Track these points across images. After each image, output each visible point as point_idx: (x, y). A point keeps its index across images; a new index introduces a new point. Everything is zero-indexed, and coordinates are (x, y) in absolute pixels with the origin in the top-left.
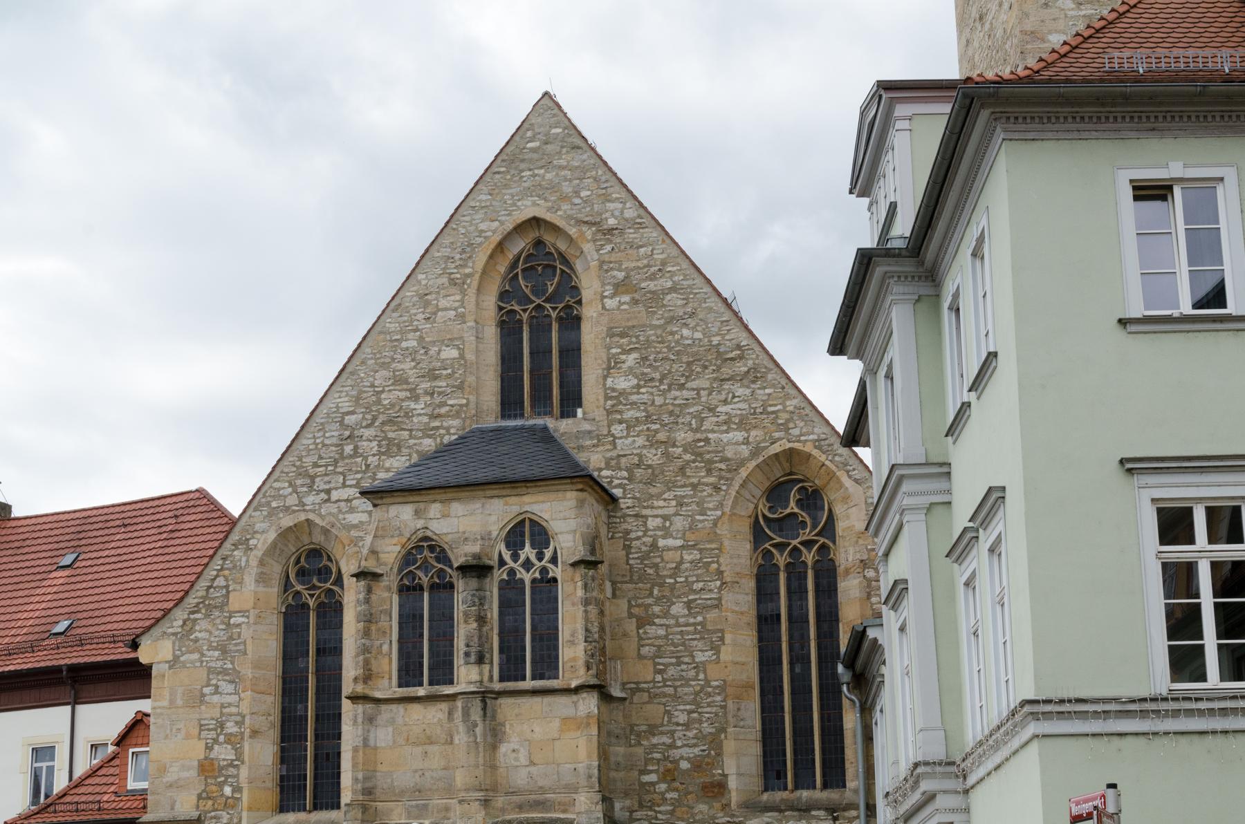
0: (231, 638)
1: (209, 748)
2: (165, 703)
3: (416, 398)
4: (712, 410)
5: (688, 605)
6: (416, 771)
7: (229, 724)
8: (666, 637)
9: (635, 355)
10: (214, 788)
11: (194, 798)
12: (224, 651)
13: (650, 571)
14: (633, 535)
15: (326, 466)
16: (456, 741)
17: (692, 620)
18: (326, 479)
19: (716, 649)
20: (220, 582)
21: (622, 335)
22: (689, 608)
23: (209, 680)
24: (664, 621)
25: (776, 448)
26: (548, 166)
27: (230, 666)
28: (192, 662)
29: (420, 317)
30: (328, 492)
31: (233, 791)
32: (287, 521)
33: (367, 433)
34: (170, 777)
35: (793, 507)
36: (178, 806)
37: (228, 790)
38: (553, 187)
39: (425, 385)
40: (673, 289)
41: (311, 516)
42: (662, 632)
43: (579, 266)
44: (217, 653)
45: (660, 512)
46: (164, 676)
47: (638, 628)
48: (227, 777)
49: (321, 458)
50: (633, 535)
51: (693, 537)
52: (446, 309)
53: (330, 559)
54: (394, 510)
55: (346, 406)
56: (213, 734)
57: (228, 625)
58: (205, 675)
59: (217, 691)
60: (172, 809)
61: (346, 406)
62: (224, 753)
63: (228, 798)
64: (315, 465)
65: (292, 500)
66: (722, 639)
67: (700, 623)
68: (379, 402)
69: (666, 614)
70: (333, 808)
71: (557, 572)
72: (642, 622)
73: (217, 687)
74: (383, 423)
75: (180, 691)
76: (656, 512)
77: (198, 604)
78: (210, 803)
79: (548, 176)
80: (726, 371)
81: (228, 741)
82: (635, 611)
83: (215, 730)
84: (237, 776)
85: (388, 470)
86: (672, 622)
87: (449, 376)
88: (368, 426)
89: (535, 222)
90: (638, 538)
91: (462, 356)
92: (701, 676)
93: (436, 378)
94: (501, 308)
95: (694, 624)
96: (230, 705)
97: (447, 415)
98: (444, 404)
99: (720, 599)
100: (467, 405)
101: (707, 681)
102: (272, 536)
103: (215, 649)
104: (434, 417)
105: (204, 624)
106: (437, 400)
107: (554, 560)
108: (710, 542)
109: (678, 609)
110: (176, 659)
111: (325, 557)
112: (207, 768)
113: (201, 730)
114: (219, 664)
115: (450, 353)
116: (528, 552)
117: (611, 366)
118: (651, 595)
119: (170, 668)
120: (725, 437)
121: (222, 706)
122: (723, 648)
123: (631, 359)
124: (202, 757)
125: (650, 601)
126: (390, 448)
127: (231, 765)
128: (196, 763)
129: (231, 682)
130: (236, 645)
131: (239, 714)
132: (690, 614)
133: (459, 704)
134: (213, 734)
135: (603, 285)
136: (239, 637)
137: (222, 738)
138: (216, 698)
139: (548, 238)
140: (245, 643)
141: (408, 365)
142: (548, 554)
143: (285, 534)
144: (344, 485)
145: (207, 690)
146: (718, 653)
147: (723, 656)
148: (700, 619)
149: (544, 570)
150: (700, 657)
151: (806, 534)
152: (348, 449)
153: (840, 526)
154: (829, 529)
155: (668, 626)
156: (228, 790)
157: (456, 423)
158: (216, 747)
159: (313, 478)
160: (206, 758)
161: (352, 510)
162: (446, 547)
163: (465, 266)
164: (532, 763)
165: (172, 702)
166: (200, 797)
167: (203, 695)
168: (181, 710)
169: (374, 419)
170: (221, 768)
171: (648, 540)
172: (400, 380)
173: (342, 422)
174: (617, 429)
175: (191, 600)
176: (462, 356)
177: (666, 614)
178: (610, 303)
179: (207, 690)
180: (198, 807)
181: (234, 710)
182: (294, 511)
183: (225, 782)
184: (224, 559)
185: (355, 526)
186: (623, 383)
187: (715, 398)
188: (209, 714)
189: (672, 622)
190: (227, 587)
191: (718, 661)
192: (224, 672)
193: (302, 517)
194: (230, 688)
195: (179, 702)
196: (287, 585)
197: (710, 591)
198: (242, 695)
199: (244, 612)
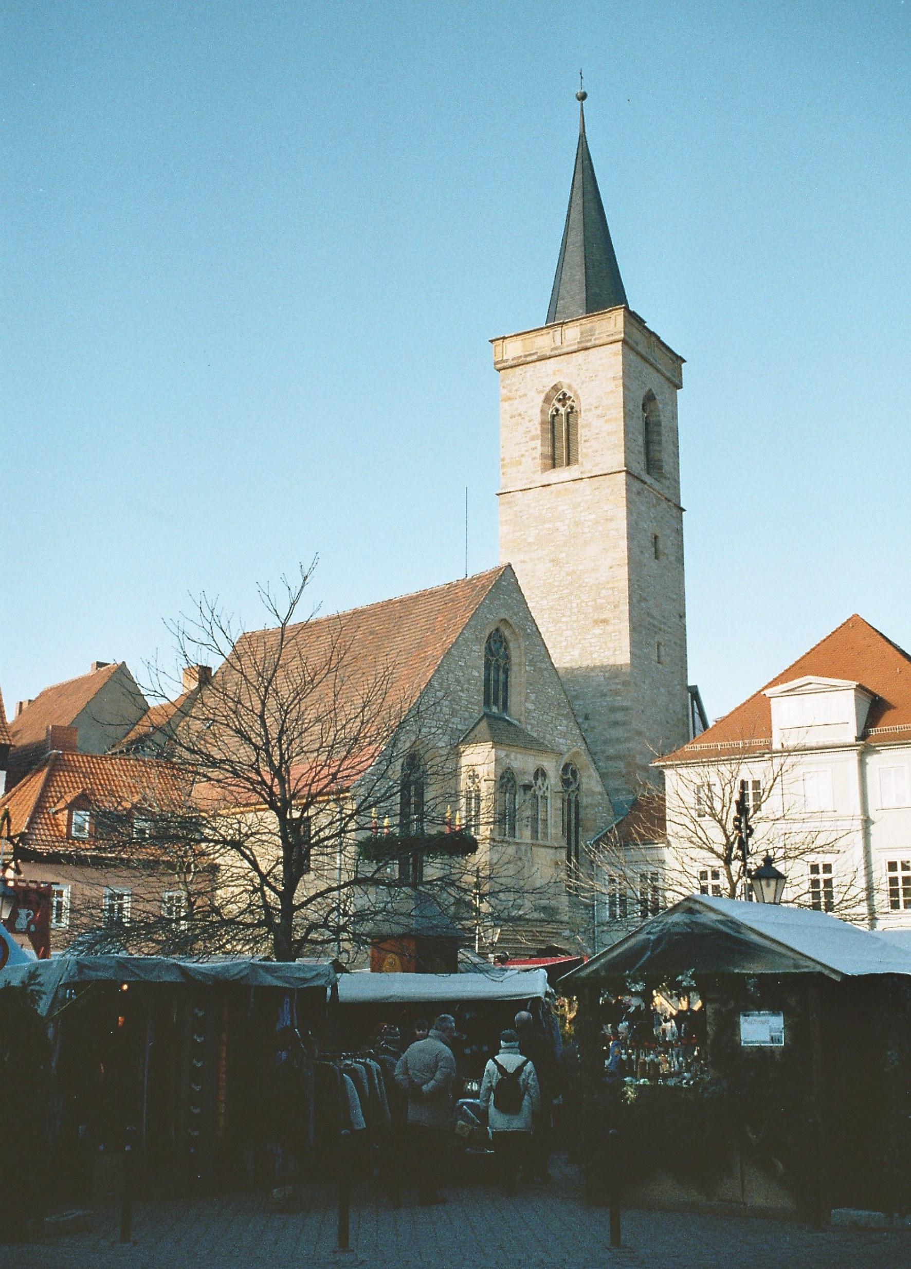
3: (462, 691)
4: (556, 727)
21: (531, 684)
26: (509, 596)
35: (570, 776)
40: (546, 669)
43: (511, 645)
54: (499, 752)
68: (449, 688)
71: (548, 794)
79: (510, 601)
89: (505, 620)
115: (476, 674)
116: (540, 782)
120: (561, 740)
123: (533, 697)
126: (454, 713)
139: (502, 628)
149: (544, 792)
151: (573, 787)
153: (584, 787)
154: (578, 789)
157: (476, 707)
174: (529, 727)
178: (528, 668)
186: (531, 706)
187: (557, 723)
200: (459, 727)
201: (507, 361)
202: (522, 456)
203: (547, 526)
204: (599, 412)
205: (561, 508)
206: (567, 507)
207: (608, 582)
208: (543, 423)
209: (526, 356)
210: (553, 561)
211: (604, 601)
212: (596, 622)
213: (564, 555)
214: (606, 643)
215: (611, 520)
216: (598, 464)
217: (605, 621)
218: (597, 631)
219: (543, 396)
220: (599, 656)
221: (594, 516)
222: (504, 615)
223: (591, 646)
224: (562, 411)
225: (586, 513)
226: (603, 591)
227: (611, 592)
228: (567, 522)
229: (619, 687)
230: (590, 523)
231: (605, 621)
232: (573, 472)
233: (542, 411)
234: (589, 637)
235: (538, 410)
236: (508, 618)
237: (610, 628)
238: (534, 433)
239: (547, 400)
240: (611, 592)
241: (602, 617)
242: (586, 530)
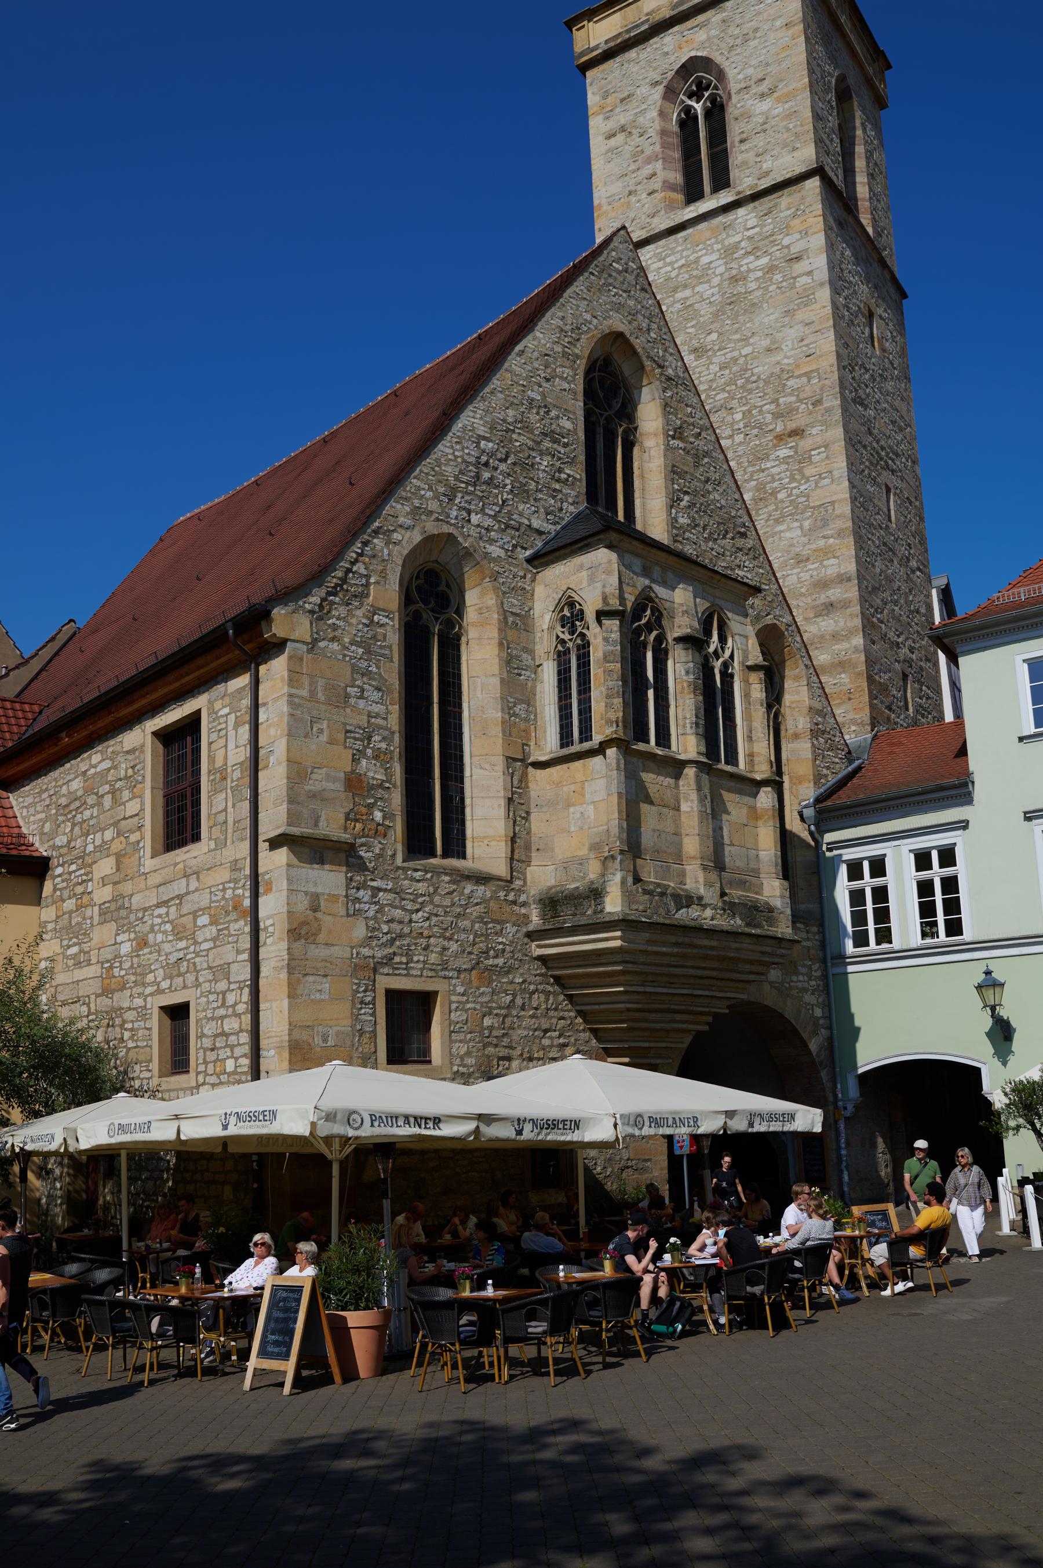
0: (374, 637)
1: (355, 760)
2: (304, 693)
6: (654, 831)
7: (377, 738)
9: (687, 498)
10: (364, 810)
11: (342, 816)
12: (368, 651)
16: (684, 807)
20: (360, 568)
23: (354, 680)
25: (769, 620)
27: (373, 669)
31: (384, 818)
34: (312, 786)
36: (322, 823)
37: (378, 816)
41: (455, 533)
44: (360, 651)
46: (301, 659)
48: (377, 799)
53: (448, 586)
56: (358, 745)
57: (372, 621)
58: (349, 673)
59: (361, 697)
60: (316, 825)
62: (371, 771)
63: (379, 824)
70: (458, 857)
75: (321, 683)
77: (337, 585)
78: (359, 826)
80: (740, 542)
81: (376, 757)
83: (362, 741)
84: (388, 801)
85: (521, 514)
102: (417, 538)
103: (358, 644)
107: (732, 657)
111: (444, 582)
112: (354, 783)
113: (346, 738)
114: (364, 664)
117: (673, 502)
119: (310, 651)
121: (369, 715)
124: (349, 769)
127: (381, 786)
128: (342, 775)
129: (378, 689)
130: (381, 647)
131: (386, 729)
133: (690, 772)
134: (358, 745)
136: (384, 640)
137: (369, 752)
138: (362, 703)
140: (390, 647)
142: (727, 654)
143: (430, 540)
145: (352, 691)
156: (378, 816)
158: (364, 762)
160: (353, 772)
162: (665, 612)
164: (732, 844)
165: (313, 692)
167: (347, 696)
168: (323, 707)
170: (372, 787)
175: (332, 581)
180: (346, 829)
181: (380, 721)
184: (366, 544)
193: (446, 529)
194: (376, 695)
195: (321, 696)
198: (390, 707)
200: (536, 524)
201: (596, 48)
202: (630, 193)
203: (679, 295)
204: (764, 87)
205: (705, 260)
206: (714, 257)
207: (798, 366)
208: (663, 133)
209: (628, 31)
210: (695, 350)
211: (793, 399)
212: (780, 438)
213: (714, 336)
214: (800, 471)
215: (798, 259)
216: (767, 173)
217: (797, 433)
218: (783, 452)
219: (661, 89)
220: (789, 496)
221: (765, 260)
223: (773, 480)
224: (698, 107)
225: (752, 258)
226: (789, 383)
227: (805, 379)
228: (716, 281)
229: (831, 541)
230: (760, 274)
231: (797, 433)
232: (725, 197)
233: (662, 114)
234: (769, 465)
235: (654, 113)
236: (627, 334)
237: (805, 444)
238: (648, 152)
239: (670, 93)
240: (805, 379)
241: (791, 426)
242: (753, 286)
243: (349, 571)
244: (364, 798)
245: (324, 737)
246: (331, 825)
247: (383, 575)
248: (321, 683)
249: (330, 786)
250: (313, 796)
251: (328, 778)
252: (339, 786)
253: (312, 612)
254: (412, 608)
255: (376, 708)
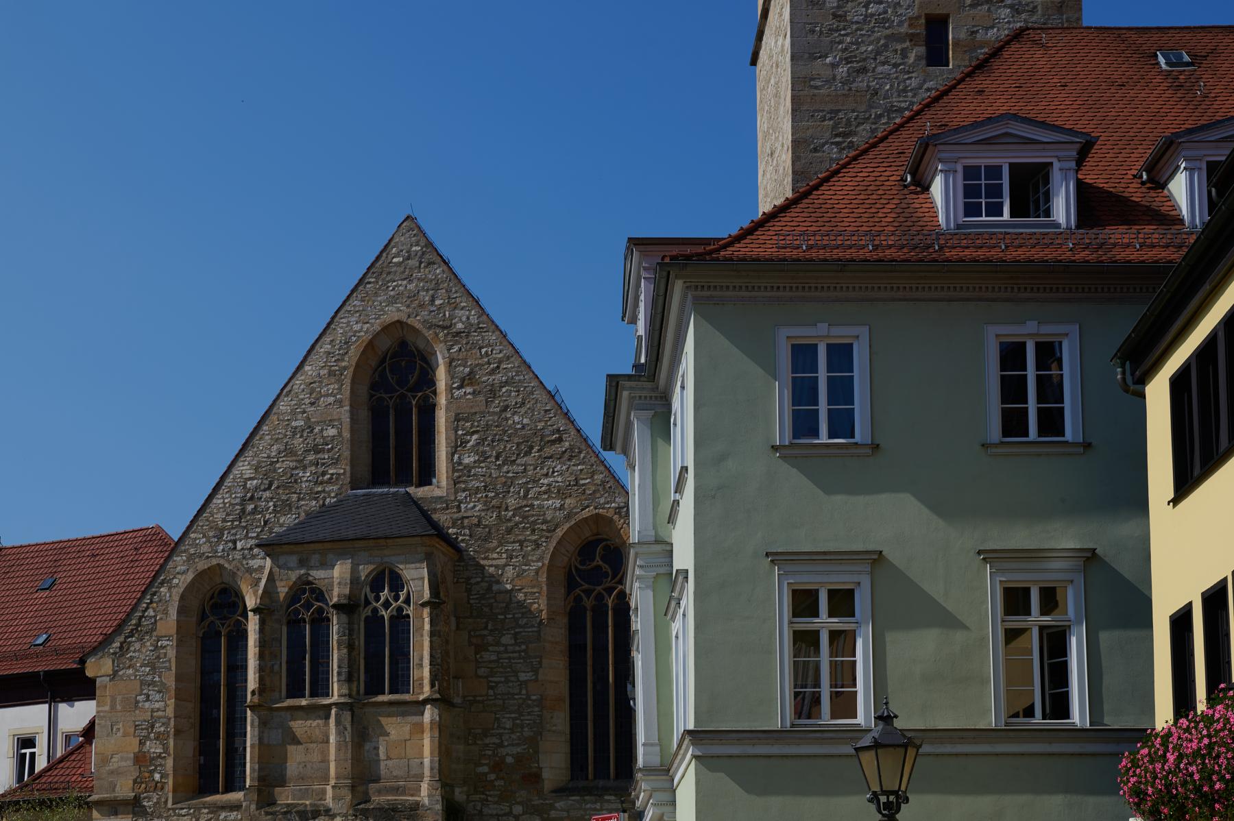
0: (158, 657)
1: (142, 743)
2: (107, 708)
5: (515, 636)
8: (497, 661)
10: (147, 775)
12: (154, 668)
13: (486, 609)
14: (473, 581)
15: (232, 521)
17: (517, 648)
18: (233, 531)
19: (536, 671)
20: (151, 612)
22: (516, 639)
24: (496, 648)
27: (157, 679)
28: (129, 676)
29: (307, 401)
30: (235, 542)
32: (202, 565)
33: (268, 494)
36: (118, 788)
37: (157, 776)
38: (413, 296)
39: (311, 457)
41: (222, 562)
42: (493, 657)
45: (495, 562)
47: (476, 653)
49: (228, 515)
50: (473, 581)
51: (519, 583)
52: (327, 395)
55: (248, 473)
59: (148, 699)
60: (114, 791)
61: (248, 473)
62: (153, 748)
64: (224, 521)
65: (205, 549)
66: (540, 663)
67: (524, 651)
68: (275, 470)
69: (498, 644)
72: (480, 648)
73: (148, 696)
74: (278, 487)
75: (119, 698)
76: (490, 562)
81: (157, 739)
82: (474, 640)
85: (281, 526)
86: (502, 649)
87: (329, 451)
88: (265, 490)
90: (478, 583)
91: (340, 434)
92: (524, 692)
93: (317, 452)
94: (372, 396)
95: (519, 652)
96: (158, 710)
97: (329, 481)
98: (324, 474)
99: (539, 632)
100: (344, 474)
101: (528, 698)
102: (190, 577)
103: (146, 665)
104: (316, 483)
105: (137, 645)
106: (321, 470)
108: (533, 587)
109: (507, 639)
110: (115, 673)
112: (141, 759)
115: (332, 432)
118: (486, 628)
121: (153, 711)
122: (541, 671)
125: (486, 632)
126: (284, 507)
127: (159, 756)
129: (159, 692)
132: (516, 644)
134: (144, 733)
135: (452, 378)
138: (147, 705)
140: (170, 661)
141: (298, 441)
143: (200, 575)
144: (247, 537)
145: (140, 698)
146: (536, 673)
147: (540, 677)
148: (523, 647)
150: (523, 677)
152: (250, 507)
155: (499, 653)
156: (157, 776)
159: (222, 531)
161: (254, 557)
163: (343, 360)
165: (113, 707)
166: (135, 782)
167: (137, 702)
169: (270, 484)
171: (484, 585)
172: (289, 452)
173: (245, 486)
175: (127, 630)
176: (340, 434)
177: (498, 644)
179: (140, 698)
181: (160, 713)
182: (208, 557)
183: (154, 771)
184: (154, 594)
185: (256, 570)
188: (142, 716)
189: (502, 649)
190: (155, 616)
191: (536, 680)
192: (153, 683)
194: (158, 697)
196: (203, 617)
197: (533, 626)
199: (169, 637)
222: (393, 313)
243: (141, 617)
244: (147, 767)
245: (120, 734)
246: (124, 790)
247: (166, 612)
248: (119, 698)
249: (124, 764)
250: (112, 772)
251: (122, 759)
252: (130, 763)
253: (115, 653)
254: (206, 623)
255: (157, 705)
